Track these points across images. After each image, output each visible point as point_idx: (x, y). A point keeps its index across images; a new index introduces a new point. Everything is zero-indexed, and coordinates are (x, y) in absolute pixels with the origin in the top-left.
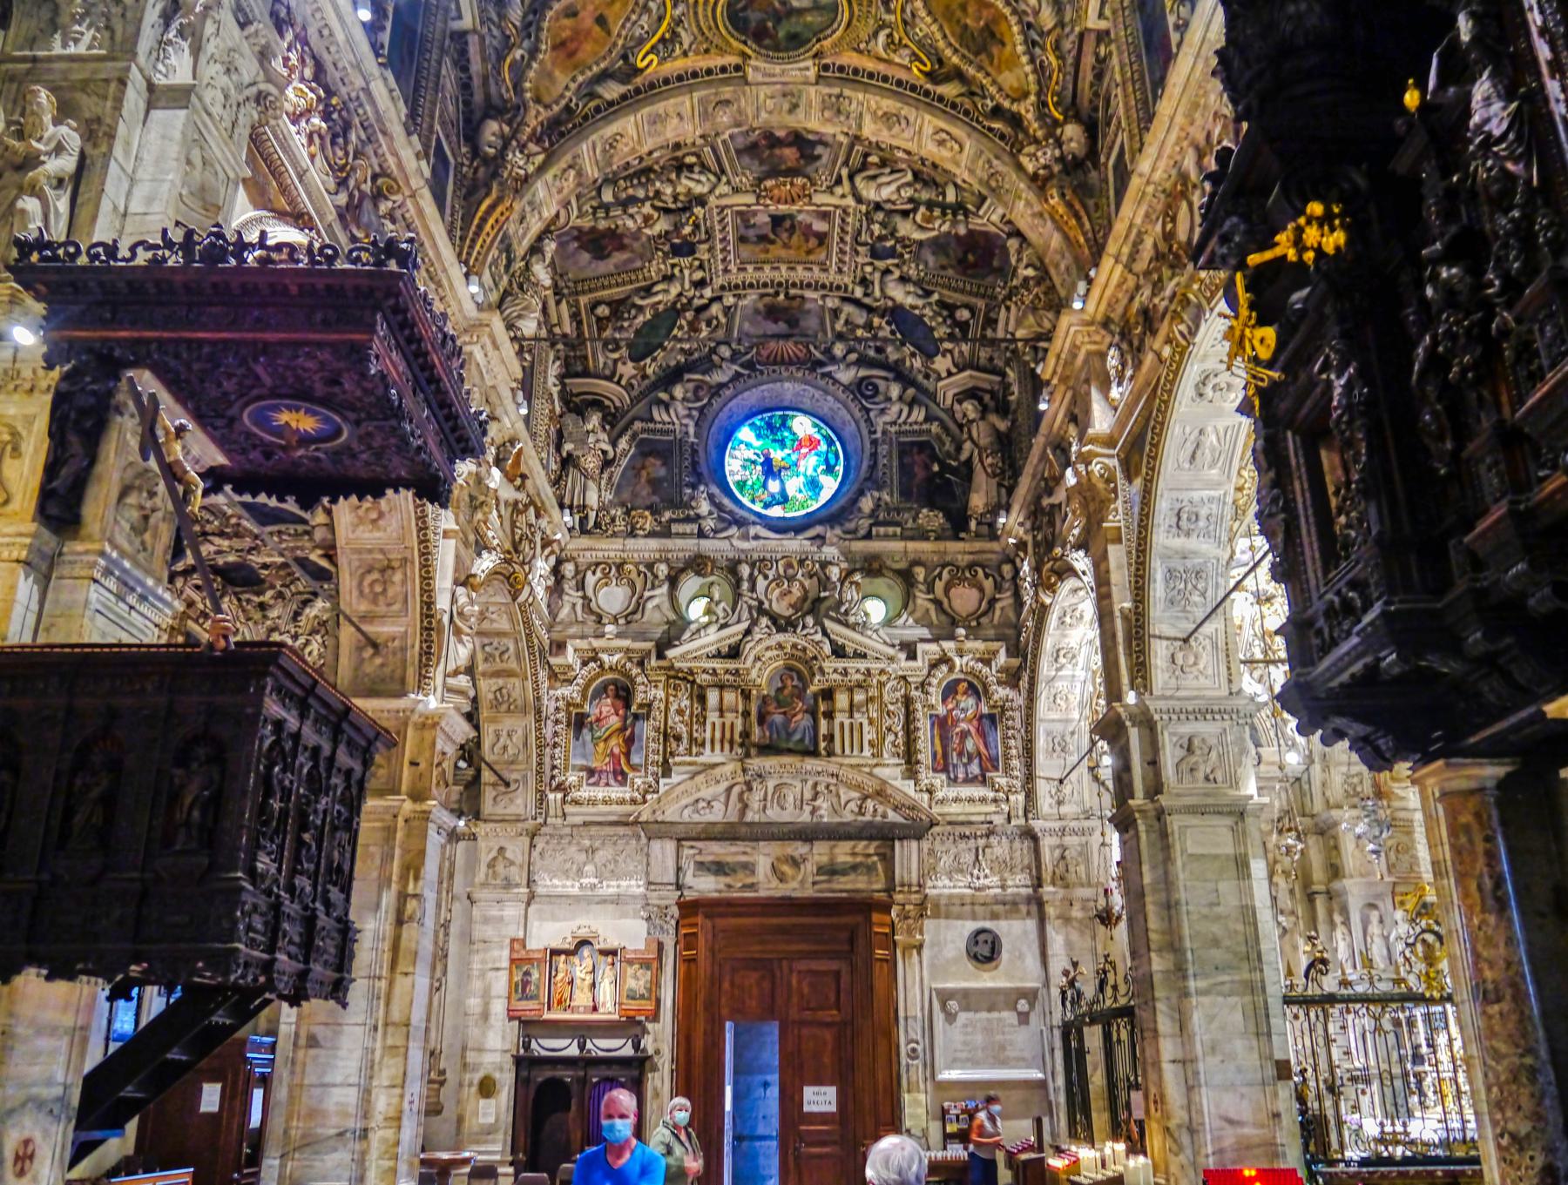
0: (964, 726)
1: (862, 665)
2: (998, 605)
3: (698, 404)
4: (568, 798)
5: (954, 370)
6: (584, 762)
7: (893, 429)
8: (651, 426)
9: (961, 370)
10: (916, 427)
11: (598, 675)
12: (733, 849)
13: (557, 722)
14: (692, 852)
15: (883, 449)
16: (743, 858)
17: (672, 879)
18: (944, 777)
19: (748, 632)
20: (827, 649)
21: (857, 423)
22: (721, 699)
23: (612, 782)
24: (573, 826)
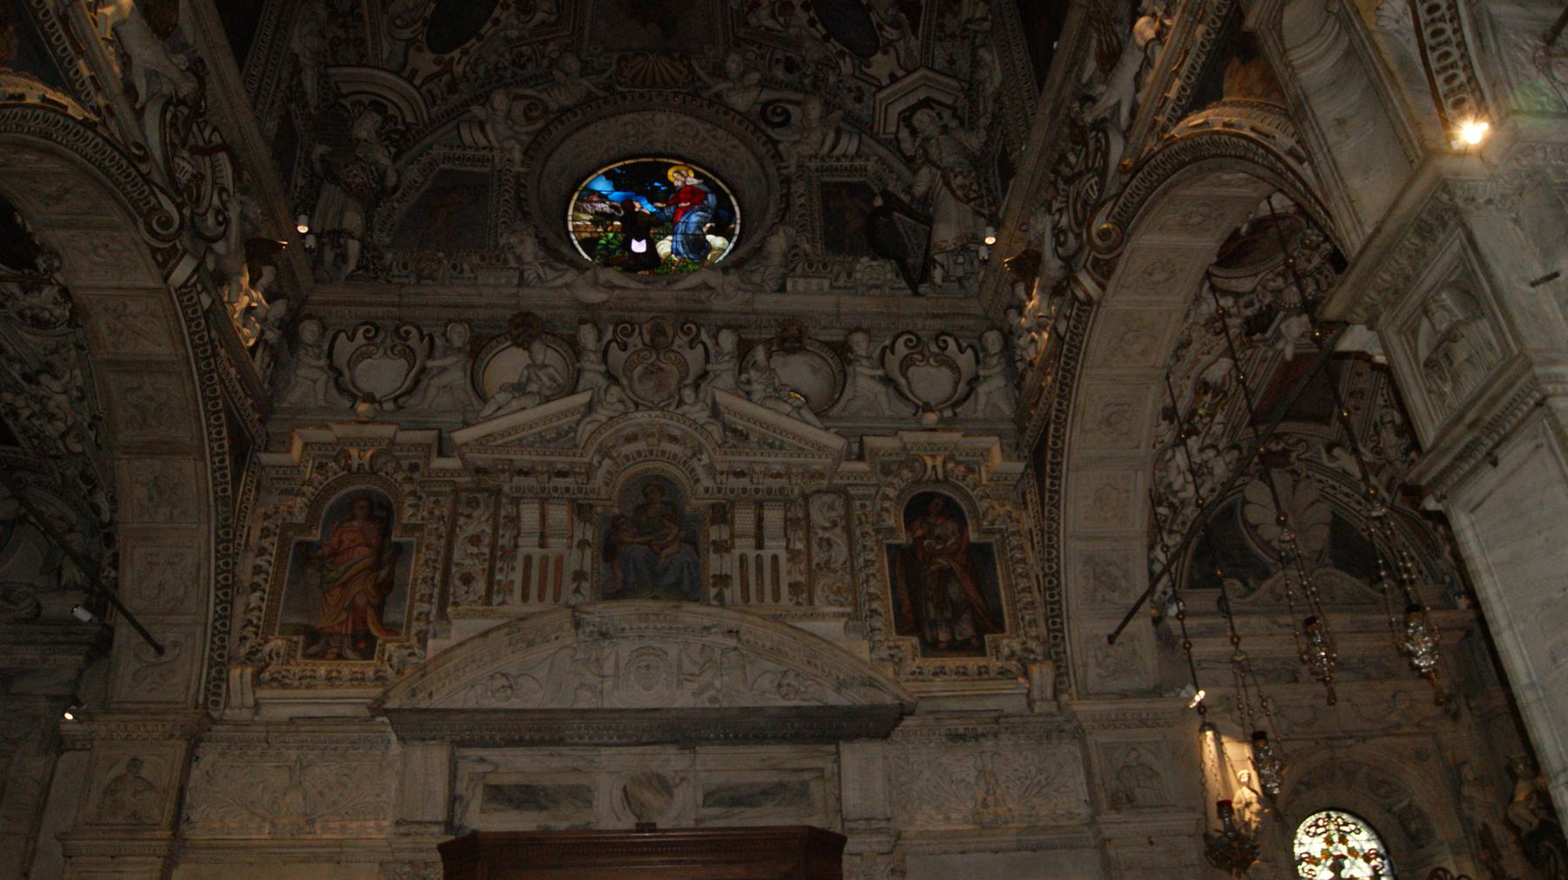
0: (942, 561)
1: (776, 462)
2: (982, 389)
3: (530, 128)
4: (266, 675)
5: (900, 73)
6: (305, 621)
7: (813, 165)
8: (459, 152)
9: (909, 73)
10: (846, 163)
11: (341, 483)
12: (556, 763)
13: (262, 552)
14: (480, 768)
15: (799, 187)
16: (572, 780)
17: (441, 815)
18: (915, 640)
19: (590, 408)
20: (716, 430)
21: (760, 160)
22: (543, 517)
23: (349, 653)
24: (268, 724)
